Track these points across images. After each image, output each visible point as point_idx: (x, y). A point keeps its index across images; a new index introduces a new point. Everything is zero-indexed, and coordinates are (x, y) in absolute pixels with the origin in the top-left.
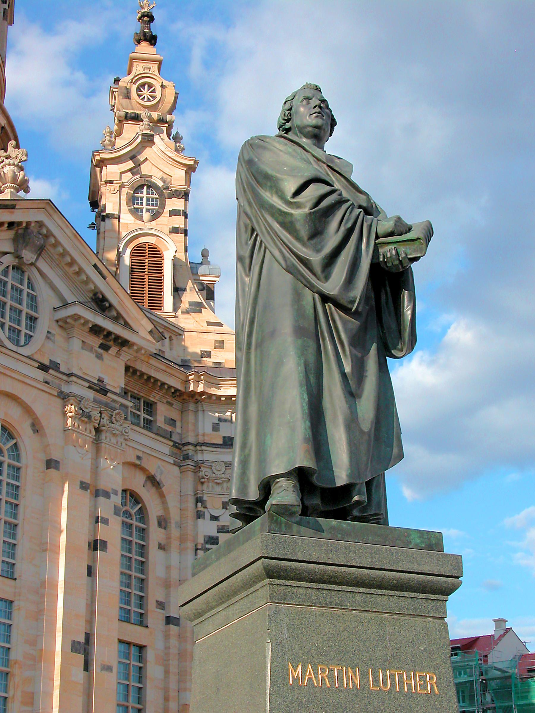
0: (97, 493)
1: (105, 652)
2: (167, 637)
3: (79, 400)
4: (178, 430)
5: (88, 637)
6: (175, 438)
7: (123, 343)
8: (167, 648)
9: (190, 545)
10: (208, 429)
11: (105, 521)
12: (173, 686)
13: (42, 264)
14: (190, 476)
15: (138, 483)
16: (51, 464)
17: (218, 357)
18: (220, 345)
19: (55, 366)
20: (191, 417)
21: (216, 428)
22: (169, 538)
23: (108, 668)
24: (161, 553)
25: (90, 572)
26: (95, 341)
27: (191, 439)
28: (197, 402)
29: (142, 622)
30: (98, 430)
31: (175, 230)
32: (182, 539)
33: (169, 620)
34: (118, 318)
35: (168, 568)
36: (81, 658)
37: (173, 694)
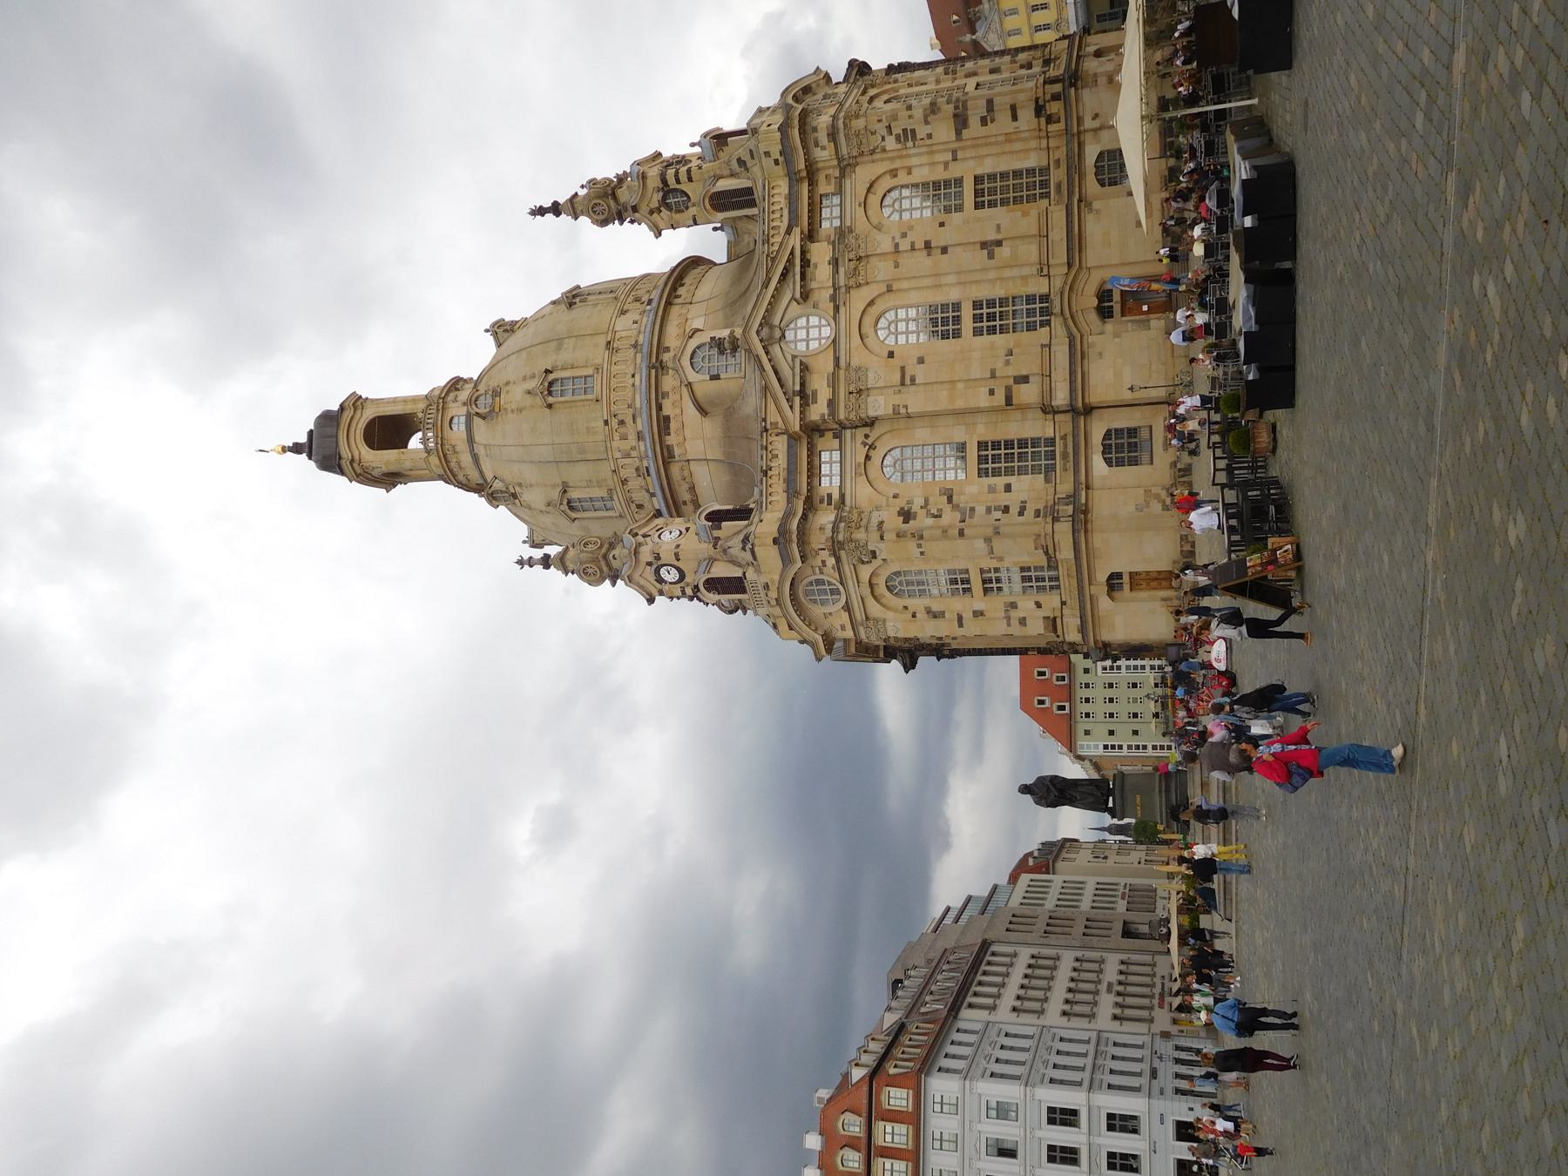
0: (897, 250)
4: (830, 171)
5: (984, 245)
7: (803, 253)
10: (825, 153)
11: (913, 244)
12: (994, 150)
13: (776, 322)
15: (874, 200)
16: (889, 290)
18: (767, 154)
19: (833, 298)
20: (820, 165)
21: (824, 148)
24: (914, 171)
25: (944, 250)
26: (809, 271)
29: (959, 182)
30: (859, 259)
31: (690, 179)
33: (955, 159)
34: (790, 261)
36: (997, 250)
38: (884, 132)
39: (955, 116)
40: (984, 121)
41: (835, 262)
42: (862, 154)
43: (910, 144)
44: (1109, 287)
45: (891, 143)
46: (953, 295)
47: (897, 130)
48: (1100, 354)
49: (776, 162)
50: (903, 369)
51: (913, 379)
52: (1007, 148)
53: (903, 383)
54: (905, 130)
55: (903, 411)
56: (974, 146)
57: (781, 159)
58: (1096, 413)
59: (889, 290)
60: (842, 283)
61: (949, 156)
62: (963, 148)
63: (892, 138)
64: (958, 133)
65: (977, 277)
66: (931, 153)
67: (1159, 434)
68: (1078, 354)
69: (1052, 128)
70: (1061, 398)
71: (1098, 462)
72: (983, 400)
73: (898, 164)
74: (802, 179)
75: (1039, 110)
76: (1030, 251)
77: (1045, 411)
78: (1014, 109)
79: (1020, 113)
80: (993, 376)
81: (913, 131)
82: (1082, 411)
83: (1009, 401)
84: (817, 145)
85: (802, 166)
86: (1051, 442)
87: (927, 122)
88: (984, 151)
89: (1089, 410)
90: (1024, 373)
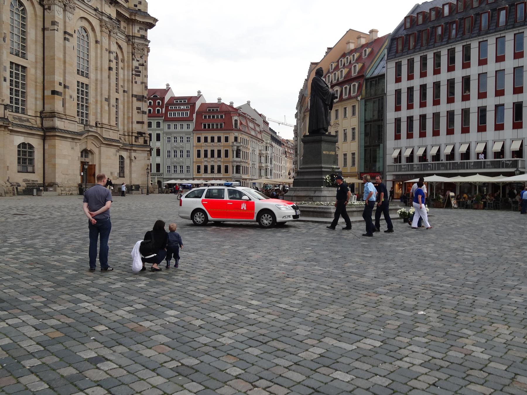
1: (113, 102)
2: (124, 96)
3: (105, 22)
5: (109, 96)
6: (126, 33)
8: (124, 99)
9: (131, 69)
10: (136, 32)
14: (131, 46)
17: (139, 7)
21: (138, 31)
22: (124, 66)
23: (113, 106)
25: (109, 77)
27: (131, 34)
28: (133, 22)
32: (128, 66)
33: (124, 91)
35: (124, 75)
37: (126, 113)
38: (141, 62)
39: (143, 96)
40: (139, 109)
41: (110, 18)
42: (134, 48)
43: (134, 73)
44: (90, 156)
45: (136, 64)
46: (92, 76)
47: (141, 68)
48: (73, 148)
49: (136, 6)
50: (71, 35)
51: (68, 40)
52: (126, 117)
53: (65, 33)
54: (140, 72)
55: (56, 27)
56: (128, 102)
57: (137, 8)
58: (41, 142)
59: (97, 42)
60: (104, 18)
61: (126, 90)
62: (128, 97)
63: (138, 66)
64: (136, 96)
65: (99, 90)
66: (128, 81)
67: (30, 177)
68: (74, 136)
69: (134, 137)
70: (58, 124)
71: (19, 139)
72: (58, 78)
73: (126, 64)
74: (130, 15)
75: (140, 134)
76: (105, 121)
77: (41, 113)
78: (142, 123)
79: (139, 125)
80: (65, 87)
81: (139, 76)
82: (48, 133)
83: (54, 92)
84: (140, 28)
85: (137, 18)
86: (24, 111)
87: (142, 83)
88: (126, 106)
89: (44, 138)
90: (67, 105)
